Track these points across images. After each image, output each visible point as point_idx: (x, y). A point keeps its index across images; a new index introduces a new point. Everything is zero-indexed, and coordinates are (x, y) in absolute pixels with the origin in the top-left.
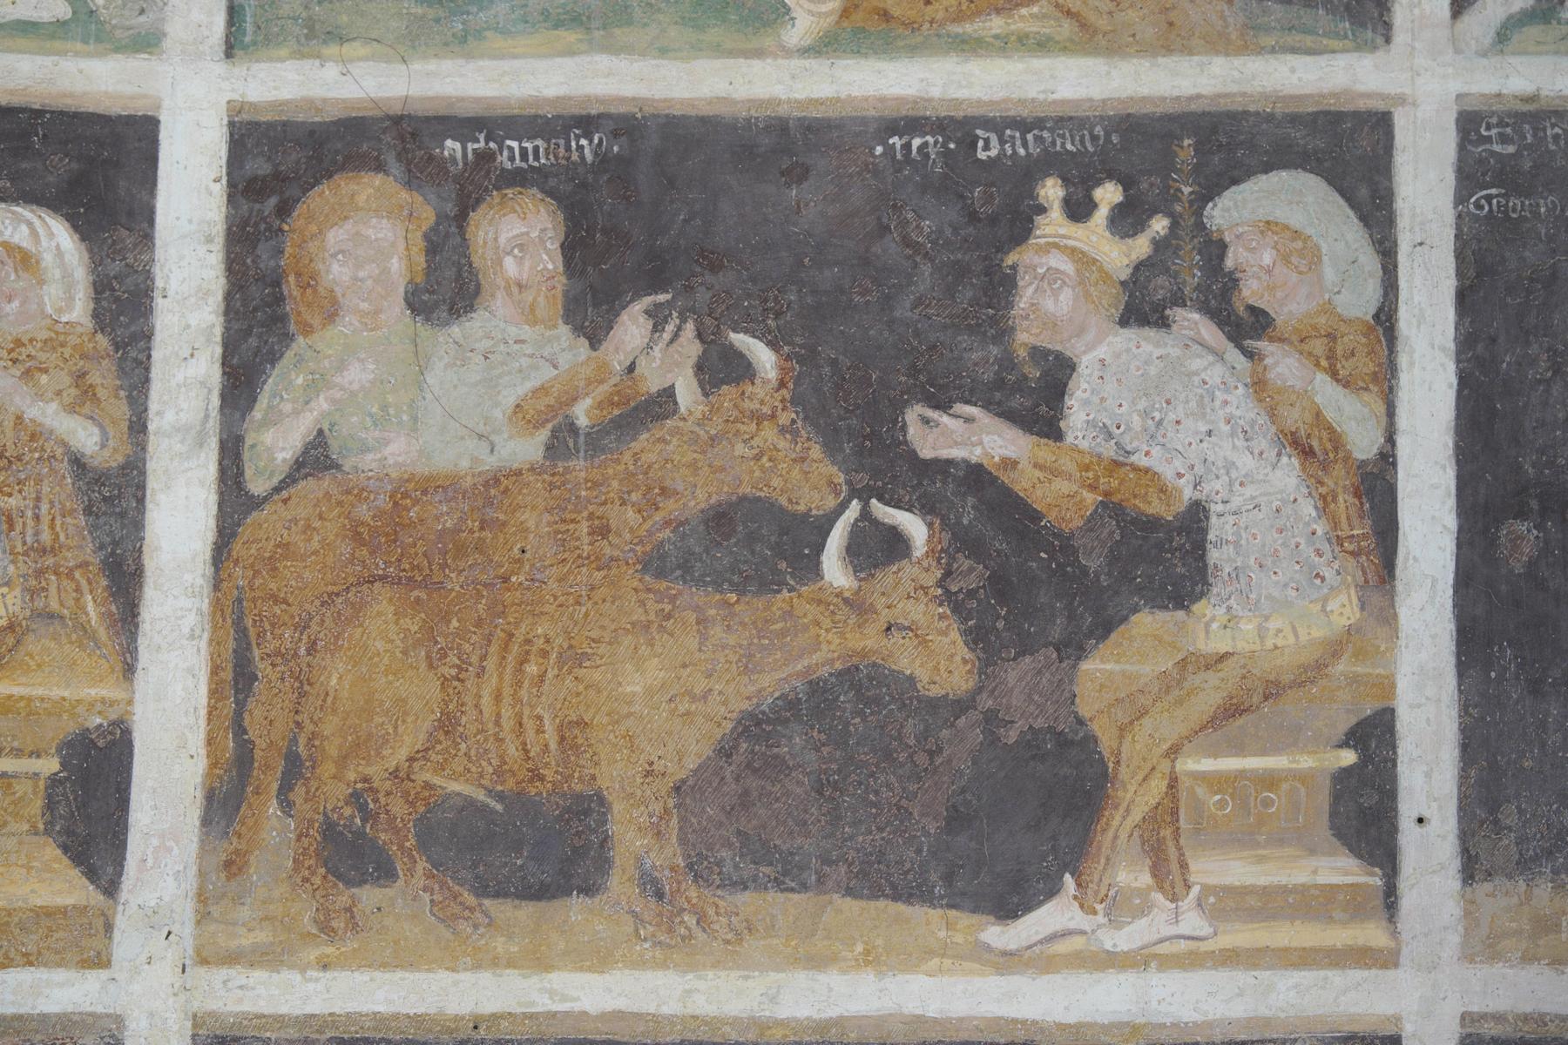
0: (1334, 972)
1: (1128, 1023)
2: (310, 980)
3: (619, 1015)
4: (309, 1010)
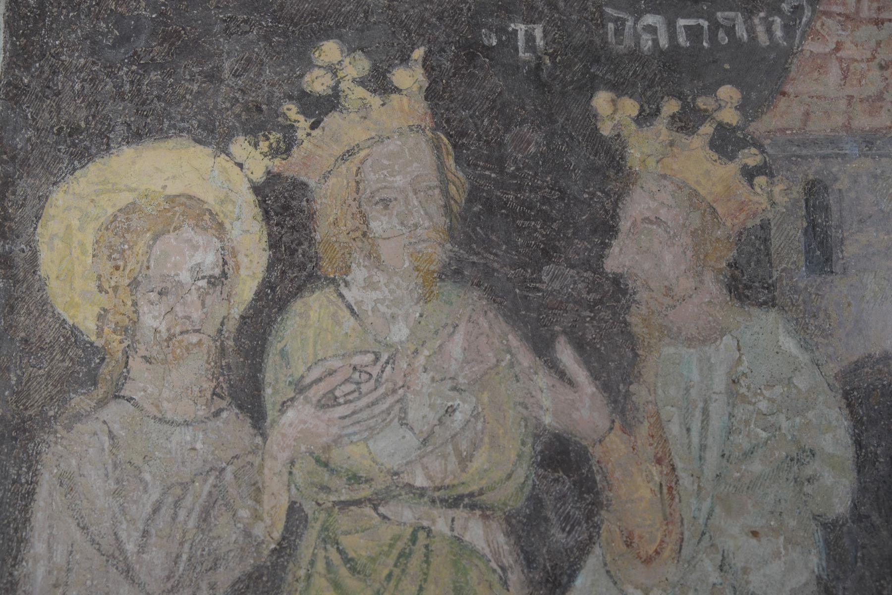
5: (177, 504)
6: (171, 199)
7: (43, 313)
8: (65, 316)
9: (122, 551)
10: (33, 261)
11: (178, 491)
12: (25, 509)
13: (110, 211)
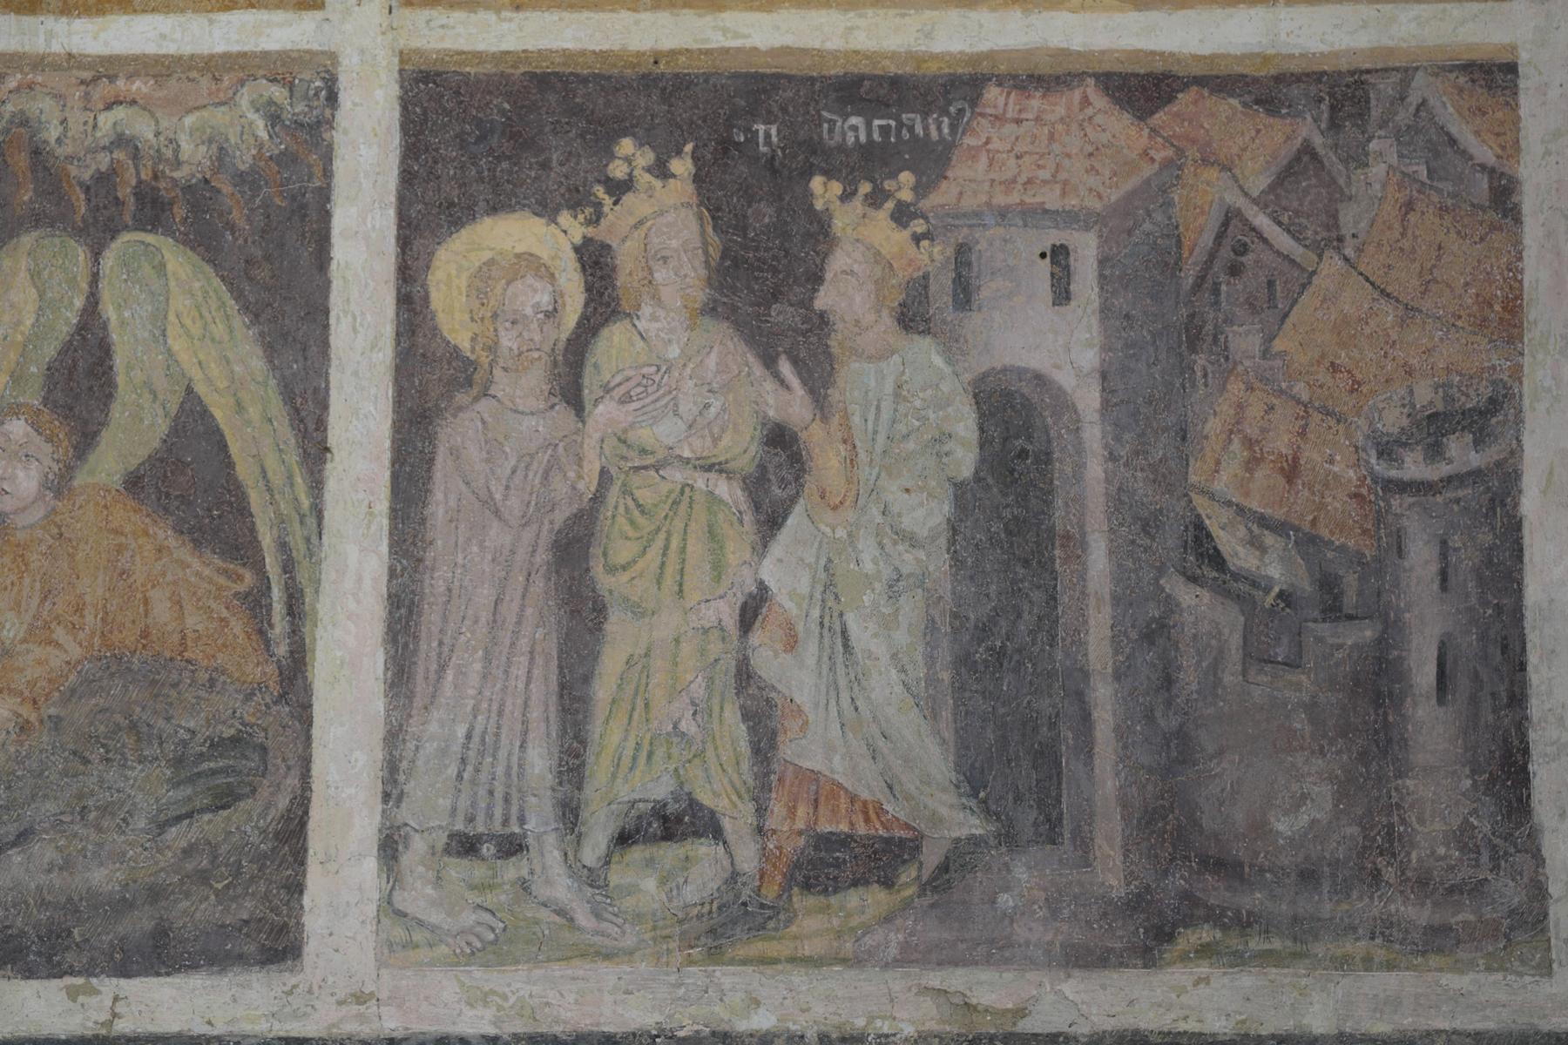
0: (1452, 5)
1: (1258, 55)
2: (504, 20)
3: (786, 51)
4: (504, 47)
5: (527, 468)
6: (518, 256)
7: (435, 336)
8: (449, 338)
9: (493, 499)
10: (426, 299)
11: (527, 459)
12: (429, 470)
13: (477, 264)
